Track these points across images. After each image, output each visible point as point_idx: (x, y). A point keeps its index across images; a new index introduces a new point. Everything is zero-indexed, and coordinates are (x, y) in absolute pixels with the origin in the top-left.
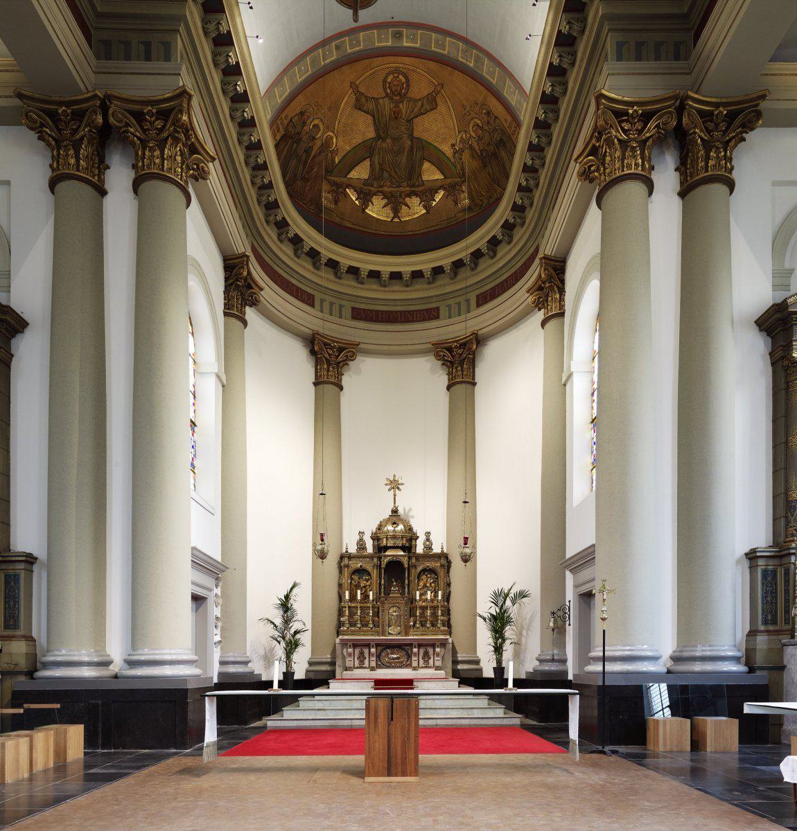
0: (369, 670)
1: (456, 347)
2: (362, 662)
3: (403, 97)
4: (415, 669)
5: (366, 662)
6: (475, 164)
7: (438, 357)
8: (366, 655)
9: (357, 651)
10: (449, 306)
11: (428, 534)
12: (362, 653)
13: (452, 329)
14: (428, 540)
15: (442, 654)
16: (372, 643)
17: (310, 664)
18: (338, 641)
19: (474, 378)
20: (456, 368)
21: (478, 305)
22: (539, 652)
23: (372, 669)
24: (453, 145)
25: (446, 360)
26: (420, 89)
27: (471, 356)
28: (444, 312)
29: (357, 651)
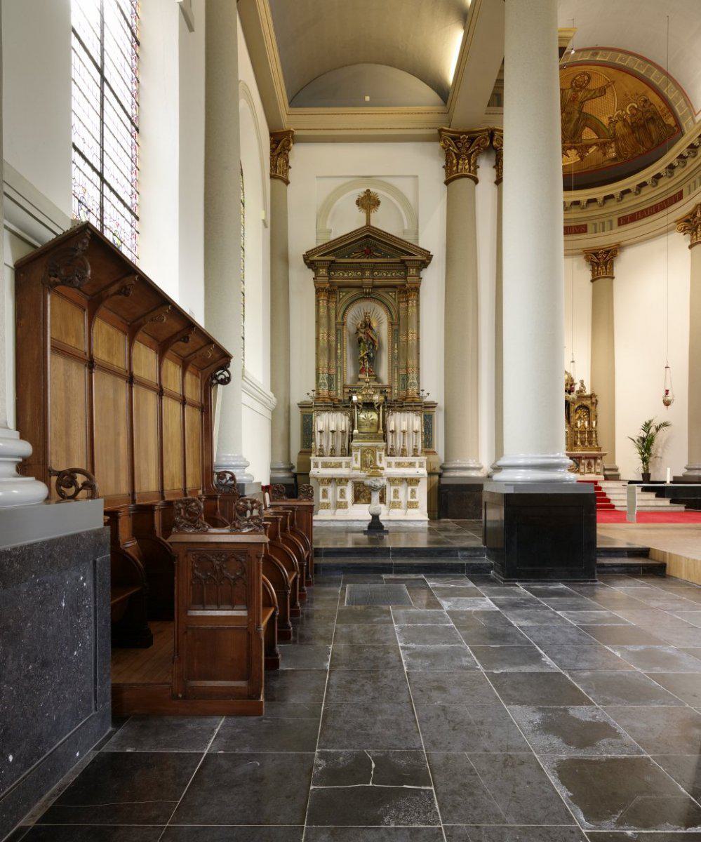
3: (582, 88)
6: (625, 131)
7: (587, 258)
10: (595, 225)
21: (619, 224)
22: (685, 463)
24: (610, 118)
26: (595, 84)
28: (590, 228)
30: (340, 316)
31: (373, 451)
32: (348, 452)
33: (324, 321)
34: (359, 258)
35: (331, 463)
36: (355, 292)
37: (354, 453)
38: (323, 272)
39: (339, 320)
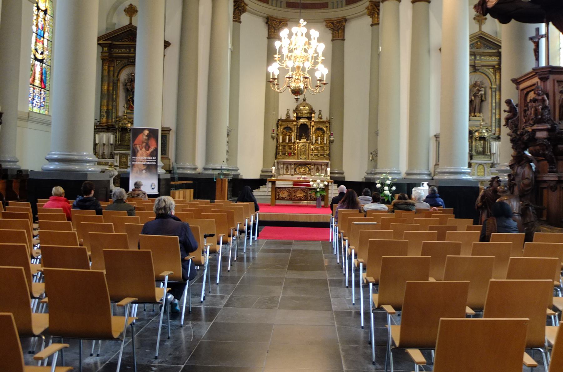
0: (290, 175)
1: (335, 23)
2: (287, 172)
4: (312, 175)
5: (289, 171)
7: (326, 26)
8: (289, 168)
9: (285, 166)
11: (320, 111)
12: (287, 168)
13: (335, 14)
14: (320, 114)
15: (325, 169)
16: (292, 163)
17: (262, 172)
18: (276, 161)
19: (344, 37)
20: (336, 32)
23: (292, 175)
25: (332, 28)
27: (342, 28)
29: (285, 166)
30: (116, 75)
31: (126, 155)
32: (112, 156)
33: (106, 78)
34: (127, 42)
35: (102, 162)
36: (125, 61)
37: (115, 157)
38: (106, 49)
39: (115, 78)
